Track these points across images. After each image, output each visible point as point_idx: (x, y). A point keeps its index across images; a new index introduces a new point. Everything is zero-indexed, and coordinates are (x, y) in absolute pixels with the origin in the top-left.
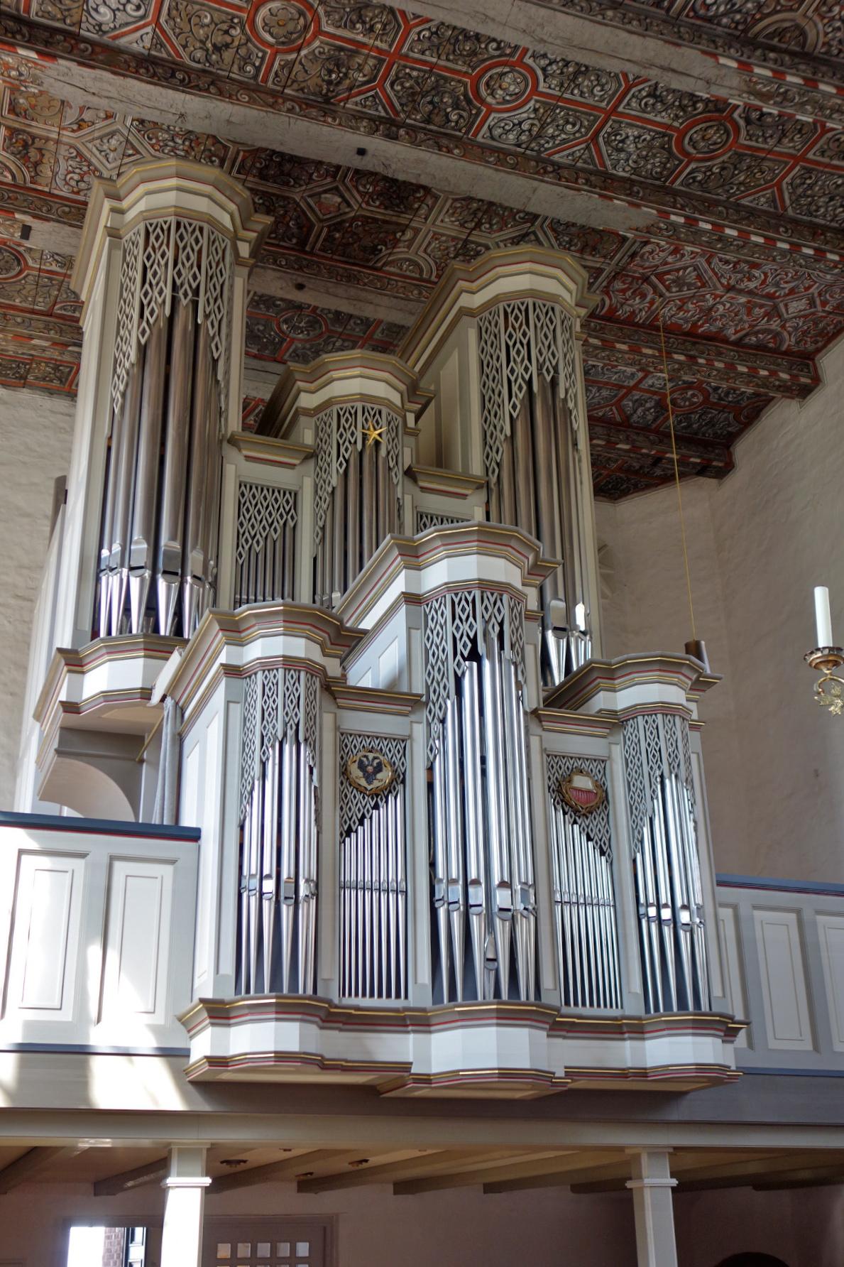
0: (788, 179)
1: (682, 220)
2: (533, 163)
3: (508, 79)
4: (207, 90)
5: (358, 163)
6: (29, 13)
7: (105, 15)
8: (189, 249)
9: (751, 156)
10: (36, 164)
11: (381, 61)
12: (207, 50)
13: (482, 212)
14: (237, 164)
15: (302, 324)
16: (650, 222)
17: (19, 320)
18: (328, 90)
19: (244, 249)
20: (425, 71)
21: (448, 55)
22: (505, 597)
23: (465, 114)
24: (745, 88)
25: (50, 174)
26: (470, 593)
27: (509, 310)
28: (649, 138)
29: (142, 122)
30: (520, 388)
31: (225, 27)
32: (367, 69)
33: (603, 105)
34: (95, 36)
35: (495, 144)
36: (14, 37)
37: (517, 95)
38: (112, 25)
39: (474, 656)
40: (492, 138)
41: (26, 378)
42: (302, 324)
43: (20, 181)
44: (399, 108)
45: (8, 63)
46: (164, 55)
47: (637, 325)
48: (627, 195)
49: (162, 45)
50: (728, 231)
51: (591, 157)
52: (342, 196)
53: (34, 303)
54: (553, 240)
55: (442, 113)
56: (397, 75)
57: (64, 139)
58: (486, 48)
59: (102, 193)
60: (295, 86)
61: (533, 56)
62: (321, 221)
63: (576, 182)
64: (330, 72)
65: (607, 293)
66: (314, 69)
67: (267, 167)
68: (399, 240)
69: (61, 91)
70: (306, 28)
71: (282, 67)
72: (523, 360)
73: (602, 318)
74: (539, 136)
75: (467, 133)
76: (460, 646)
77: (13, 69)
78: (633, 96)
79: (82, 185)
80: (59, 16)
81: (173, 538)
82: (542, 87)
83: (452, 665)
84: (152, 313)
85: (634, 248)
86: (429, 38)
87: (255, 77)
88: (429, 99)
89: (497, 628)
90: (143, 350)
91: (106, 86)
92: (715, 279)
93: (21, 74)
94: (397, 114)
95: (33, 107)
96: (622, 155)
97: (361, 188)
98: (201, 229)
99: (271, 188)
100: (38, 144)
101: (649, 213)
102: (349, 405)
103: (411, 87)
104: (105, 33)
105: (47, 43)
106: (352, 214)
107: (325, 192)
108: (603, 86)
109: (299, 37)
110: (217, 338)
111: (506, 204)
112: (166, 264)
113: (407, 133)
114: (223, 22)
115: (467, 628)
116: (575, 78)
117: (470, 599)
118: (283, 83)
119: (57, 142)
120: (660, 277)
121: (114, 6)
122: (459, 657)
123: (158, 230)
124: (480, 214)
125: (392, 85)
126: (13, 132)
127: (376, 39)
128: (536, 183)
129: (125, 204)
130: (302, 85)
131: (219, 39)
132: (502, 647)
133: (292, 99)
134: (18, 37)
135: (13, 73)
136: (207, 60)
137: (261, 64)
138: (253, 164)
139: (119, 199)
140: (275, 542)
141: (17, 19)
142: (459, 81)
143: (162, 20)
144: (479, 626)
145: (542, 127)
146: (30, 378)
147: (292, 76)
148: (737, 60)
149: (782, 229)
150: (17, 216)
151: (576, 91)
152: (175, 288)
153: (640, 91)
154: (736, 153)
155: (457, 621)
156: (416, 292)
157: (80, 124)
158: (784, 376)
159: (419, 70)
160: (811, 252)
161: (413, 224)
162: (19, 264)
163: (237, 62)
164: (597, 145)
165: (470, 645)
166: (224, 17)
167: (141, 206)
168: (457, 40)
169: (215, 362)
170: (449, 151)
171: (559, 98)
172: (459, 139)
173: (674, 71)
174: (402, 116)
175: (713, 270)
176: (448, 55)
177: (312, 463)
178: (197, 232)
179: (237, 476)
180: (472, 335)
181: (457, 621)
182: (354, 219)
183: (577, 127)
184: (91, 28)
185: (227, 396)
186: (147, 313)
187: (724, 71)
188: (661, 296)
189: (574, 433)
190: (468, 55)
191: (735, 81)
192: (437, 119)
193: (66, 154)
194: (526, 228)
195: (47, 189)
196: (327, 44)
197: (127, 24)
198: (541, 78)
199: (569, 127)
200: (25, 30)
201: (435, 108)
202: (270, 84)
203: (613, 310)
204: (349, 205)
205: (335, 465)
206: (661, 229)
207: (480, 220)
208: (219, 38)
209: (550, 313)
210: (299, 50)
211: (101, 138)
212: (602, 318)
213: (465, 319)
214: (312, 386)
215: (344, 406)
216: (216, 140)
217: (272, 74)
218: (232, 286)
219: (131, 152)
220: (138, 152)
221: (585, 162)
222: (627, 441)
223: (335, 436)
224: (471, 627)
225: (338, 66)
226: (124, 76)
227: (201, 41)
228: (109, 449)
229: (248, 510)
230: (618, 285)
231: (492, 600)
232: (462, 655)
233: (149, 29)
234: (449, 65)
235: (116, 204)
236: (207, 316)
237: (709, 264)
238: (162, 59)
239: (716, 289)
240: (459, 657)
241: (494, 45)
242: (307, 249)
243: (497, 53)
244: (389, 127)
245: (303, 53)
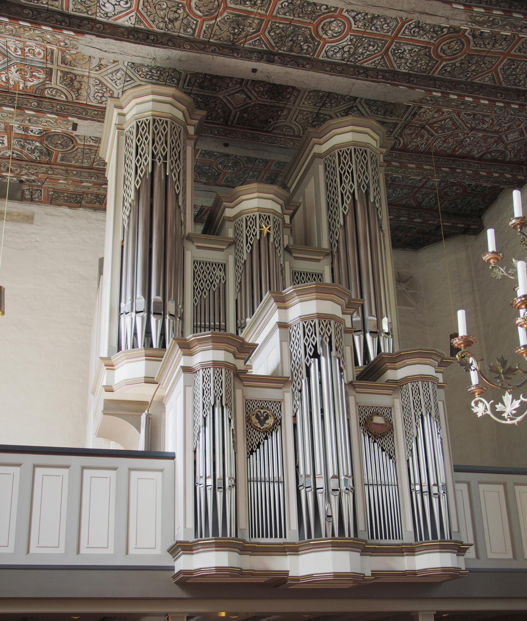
0: (501, 66)
1: (440, 95)
2: (352, 69)
3: (334, 24)
4: (167, 44)
5: (253, 76)
6: (68, 10)
7: (109, 8)
8: (160, 134)
9: (478, 55)
10: (78, 90)
11: (262, 21)
12: (166, 22)
13: (326, 98)
14: (187, 81)
15: (230, 164)
16: (421, 97)
17: (75, 173)
18: (234, 38)
19: (191, 130)
20: (287, 24)
21: (299, 14)
22: (332, 322)
23: (311, 45)
24: (470, 20)
25: (86, 94)
26: (312, 321)
27: (341, 154)
28: (417, 50)
29: (133, 63)
30: (348, 198)
31: (174, 9)
32: (254, 25)
33: (390, 34)
34: (105, 20)
35: (329, 60)
36: (61, 25)
37: (340, 33)
38: (113, 13)
39: (316, 355)
40: (328, 57)
41: (81, 203)
42: (230, 164)
43: (70, 99)
44: (274, 45)
45: (59, 39)
46: (143, 27)
47: (420, 152)
48: (407, 83)
49: (141, 22)
50: (467, 99)
51: (385, 63)
52: (246, 94)
53: (82, 162)
54: (368, 110)
55: (298, 46)
56: (271, 27)
57: (92, 75)
58: (320, 9)
59: (112, 105)
60: (215, 37)
61: (347, 11)
62: (235, 108)
63: (377, 78)
64: (234, 29)
65: (401, 137)
66: (225, 28)
67: (203, 82)
68: (280, 116)
69: (87, 51)
70: (219, 6)
71: (208, 28)
72: (349, 181)
73: (400, 150)
74: (354, 54)
75: (313, 55)
76: (308, 350)
77: (61, 41)
78: (406, 28)
79: (103, 99)
80: (85, 11)
81: (158, 294)
82: (354, 27)
83: (304, 361)
84: (142, 172)
85: (414, 111)
86: (288, 6)
87: (193, 34)
88: (290, 38)
89: (328, 340)
90: (138, 192)
91: (112, 47)
92: (463, 124)
93: (66, 44)
94: (273, 48)
95: (74, 60)
96: (403, 61)
97: (256, 89)
98: (167, 122)
99: (207, 93)
100: (78, 79)
101: (419, 93)
102: (252, 214)
103: (280, 33)
104: (110, 17)
105: (79, 26)
106: (253, 104)
107: (237, 92)
108: (388, 24)
109: (216, 11)
110: (178, 183)
111: (338, 93)
112: (148, 143)
113: (279, 58)
114: (174, 7)
115: (311, 340)
116: (372, 21)
117: (313, 324)
118: (208, 37)
119: (89, 77)
120: (431, 125)
121: (114, 3)
122: (308, 356)
123: (143, 124)
124: (324, 99)
125: (269, 32)
126: (65, 73)
127: (258, 9)
128: (354, 80)
129: (125, 111)
130: (219, 36)
131: (172, 16)
132: (331, 350)
133: (214, 44)
134: (63, 24)
135: (62, 44)
136: (166, 28)
137: (196, 27)
138: (196, 81)
139: (122, 108)
140: (214, 292)
141: (62, 14)
142: (306, 28)
143: (140, 8)
144: (318, 339)
145: (355, 49)
146: (83, 202)
147: (213, 32)
148: (464, 5)
149: (499, 95)
150: (70, 118)
151: (373, 28)
152: (153, 156)
153: (410, 25)
154: (468, 54)
155: (306, 336)
156: (291, 143)
157: (100, 66)
158: (509, 176)
159: (283, 24)
160: (517, 107)
161: (287, 106)
162: (73, 143)
163: (182, 27)
164: (388, 55)
165: (313, 349)
166: (174, 4)
167: (134, 112)
168: (304, 6)
169: (177, 195)
170: (304, 66)
171: (364, 32)
172: (310, 59)
173: (427, 14)
174: (276, 49)
175: (461, 119)
176: (299, 14)
177: (232, 248)
178: (165, 124)
179: (192, 257)
180: (321, 168)
181: (306, 336)
182: (254, 106)
183: (375, 48)
184: (102, 15)
185: (185, 214)
186: (139, 171)
187: (456, 11)
188: (432, 135)
189: (380, 221)
190: (310, 14)
191: (464, 16)
192: (296, 49)
193: (94, 83)
194: (349, 106)
195: (85, 102)
196: (231, 14)
197: (121, 12)
198: (353, 22)
199: (371, 48)
200: (67, 20)
201: (294, 43)
202: (201, 37)
203: (405, 145)
204: (250, 99)
205: (245, 248)
206: (428, 100)
207: (325, 102)
208: (172, 16)
209: (364, 154)
210: (216, 18)
211: (112, 73)
212: (400, 150)
213: (317, 160)
214: (232, 205)
215: (249, 215)
216: (175, 70)
217: (202, 32)
218: (185, 152)
219: (128, 79)
220: (132, 79)
221: (382, 66)
222: (420, 217)
223: (245, 232)
224: (314, 339)
225: (238, 25)
226: (121, 40)
227: (162, 18)
228: (122, 247)
229: (199, 276)
230: (407, 131)
231: (325, 324)
232: (309, 355)
233: (133, 14)
234: (300, 19)
235: (120, 111)
236: (172, 171)
237: (459, 117)
238: (141, 29)
239: (465, 130)
240: (308, 356)
241: (325, 7)
242: (229, 124)
243: (326, 11)
244: (269, 57)
245: (218, 19)
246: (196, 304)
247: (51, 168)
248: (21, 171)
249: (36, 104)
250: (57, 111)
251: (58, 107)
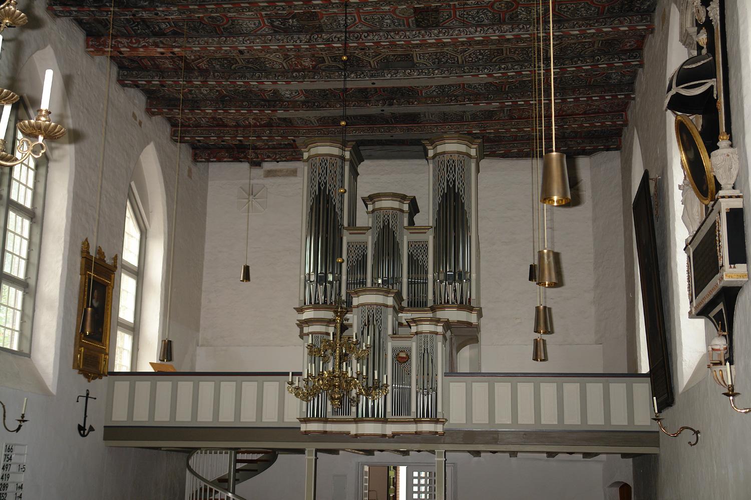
36: (264, 108)
48: (486, 100)
113: (397, 101)
246: (349, 270)
247: (295, 151)
248: (276, 156)
249: (268, 132)
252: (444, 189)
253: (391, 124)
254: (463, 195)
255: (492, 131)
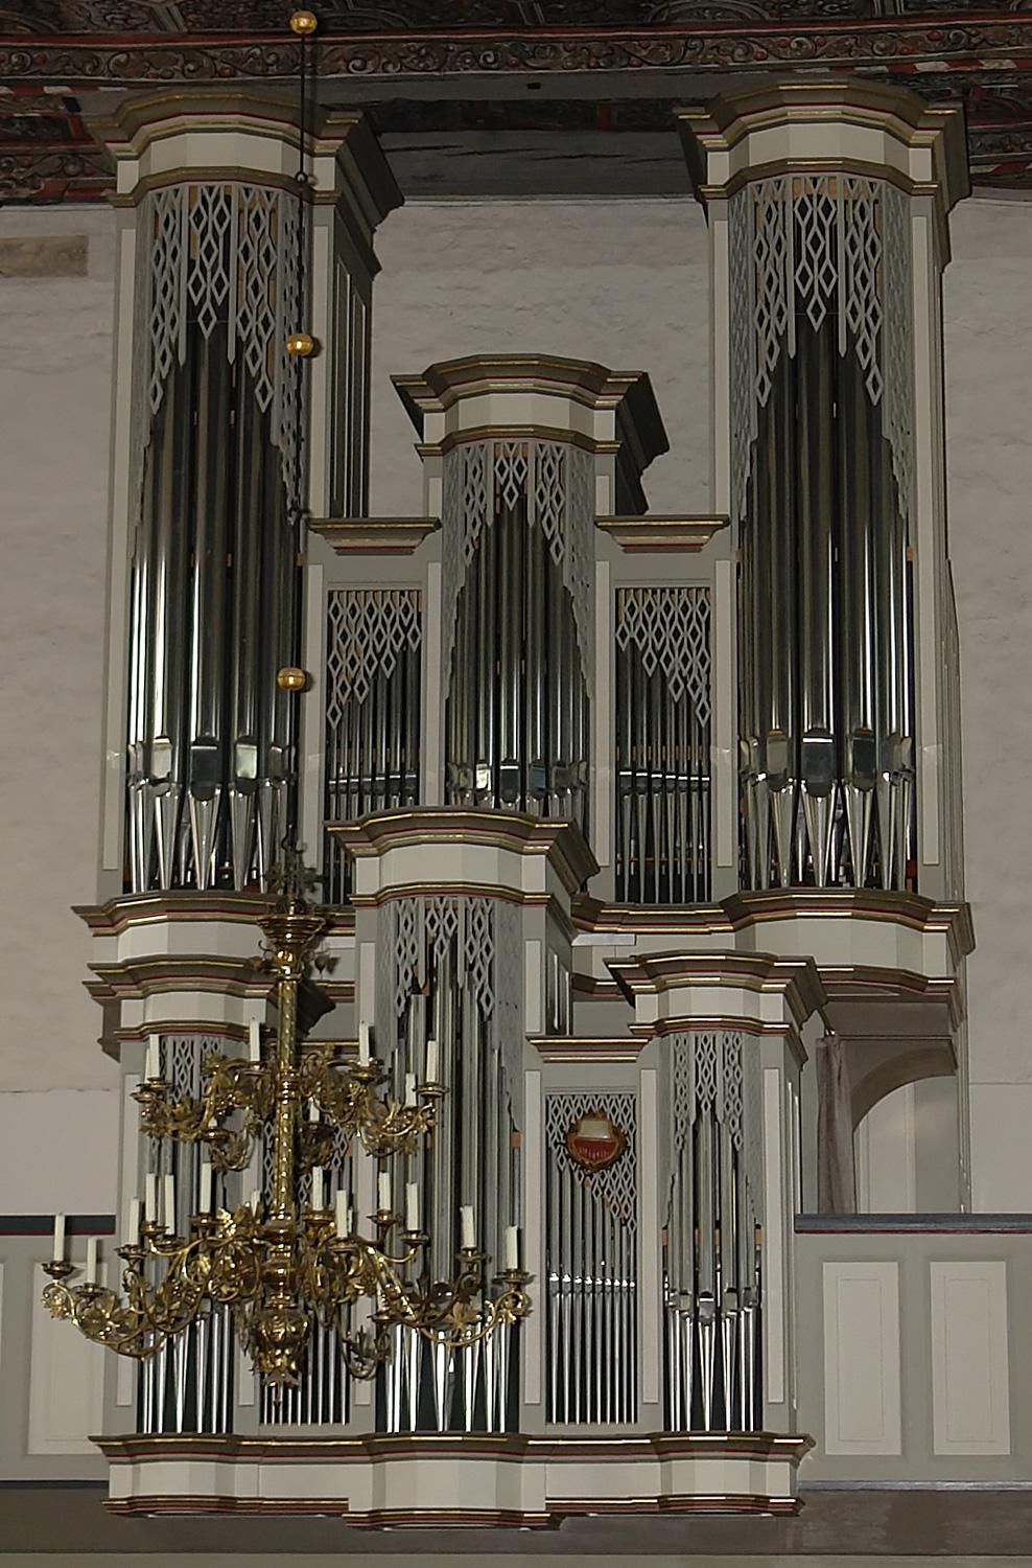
140: (389, 681)
246: (334, 725)
247: (75, 154)
250: (12, 73)
251: (14, 59)
252: (782, 339)
253: (528, 29)
254: (875, 369)
255: (1008, 64)
